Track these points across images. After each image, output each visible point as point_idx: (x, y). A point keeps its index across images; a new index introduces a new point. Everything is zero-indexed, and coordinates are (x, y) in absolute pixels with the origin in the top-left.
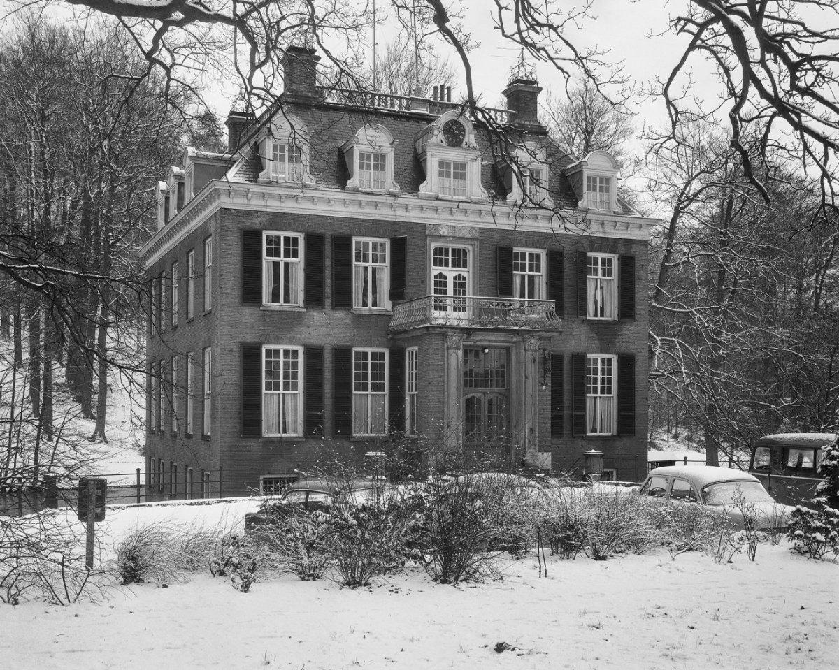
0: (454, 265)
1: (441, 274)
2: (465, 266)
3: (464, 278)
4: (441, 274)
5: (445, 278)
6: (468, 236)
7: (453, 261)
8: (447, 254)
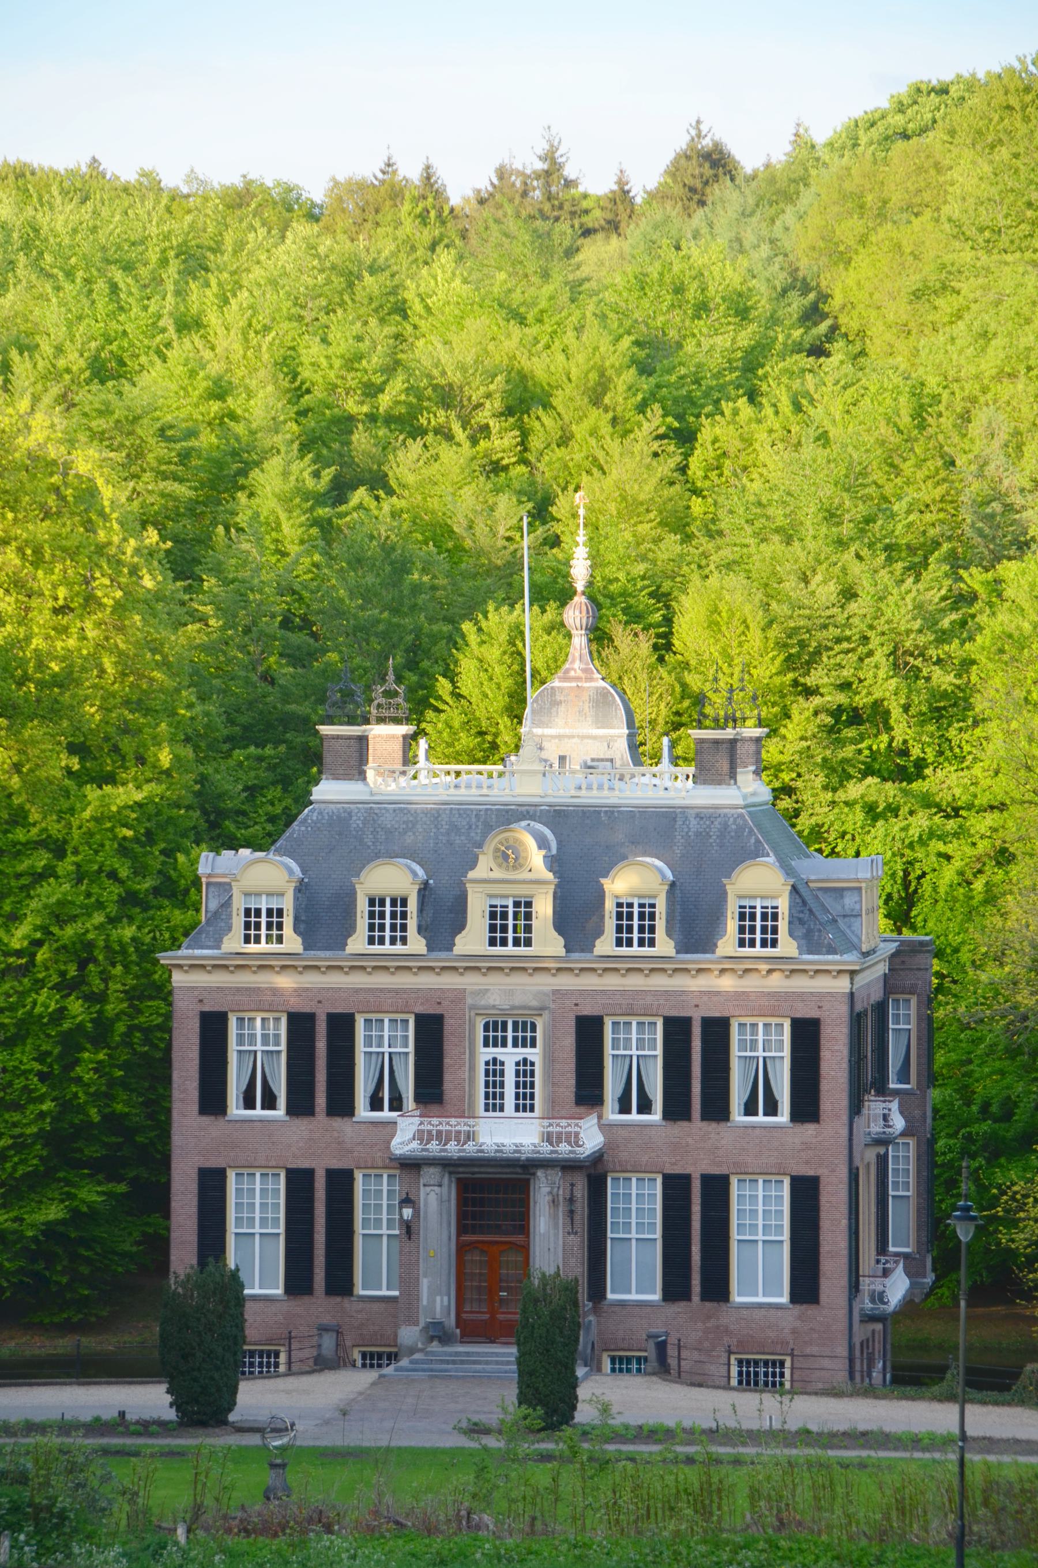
0: (515, 1045)
1: (495, 1060)
2: (533, 1045)
3: (532, 1064)
4: (495, 1060)
5: (502, 1064)
6: (534, 1003)
7: (515, 1039)
8: (504, 1029)
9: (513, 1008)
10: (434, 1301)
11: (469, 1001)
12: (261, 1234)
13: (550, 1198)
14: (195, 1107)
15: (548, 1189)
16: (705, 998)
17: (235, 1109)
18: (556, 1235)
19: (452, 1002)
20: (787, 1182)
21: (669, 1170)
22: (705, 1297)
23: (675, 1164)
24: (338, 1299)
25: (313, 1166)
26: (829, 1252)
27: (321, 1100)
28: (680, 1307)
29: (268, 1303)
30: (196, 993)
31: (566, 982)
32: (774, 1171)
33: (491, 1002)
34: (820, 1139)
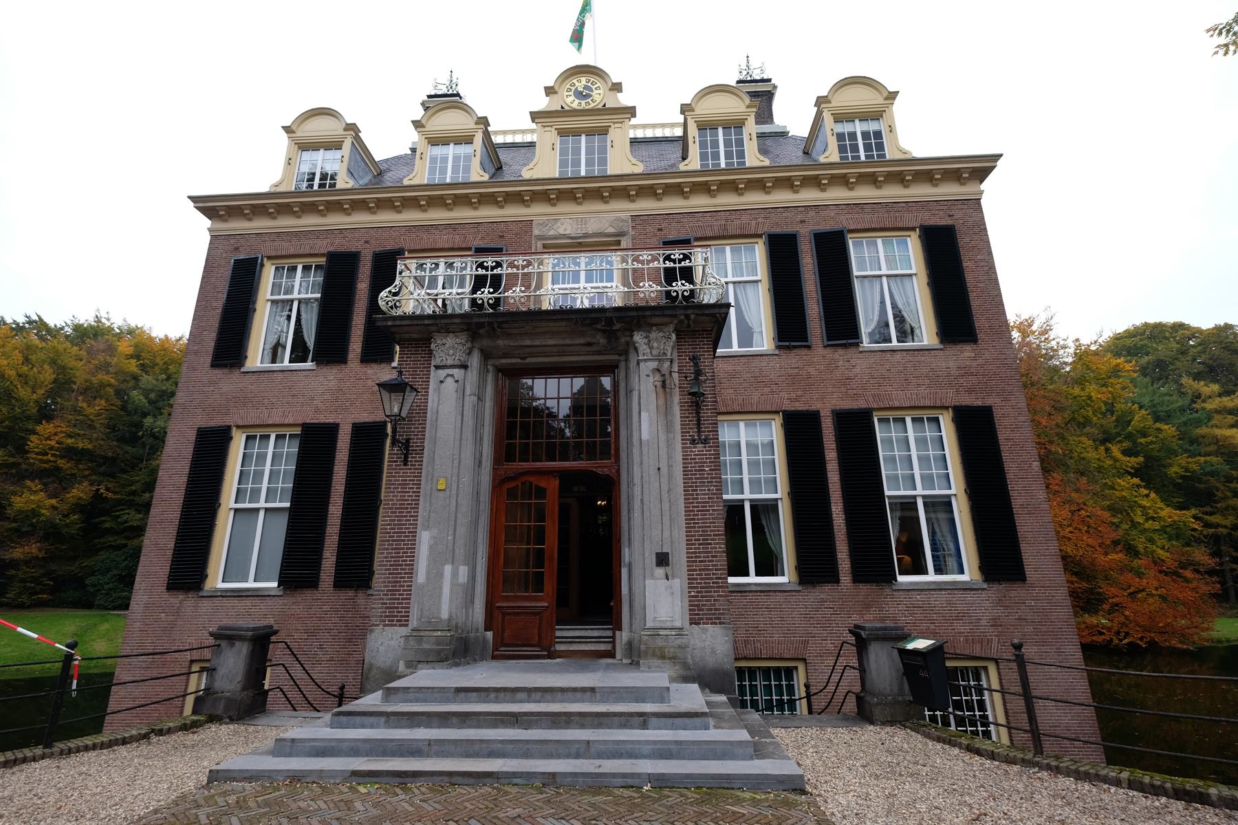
6: (611, 230)
9: (586, 236)
10: (440, 575)
11: (536, 232)
12: (267, 510)
13: (658, 377)
14: (208, 360)
15: (654, 365)
16: (812, 213)
17: (256, 357)
18: (669, 444)
19: (516, 235)
20: (946, 421)
21: (789, 406)
22: (859, 577)
23: (796, 400)
24: (351, 593)
25: (338, 421)
26: (1022, 506)
27: (356, 346)
28: (823, 592)
29: (257, 600)
30: (232, 241)
31: (646, 206)
32: (927, 403)
33: (561, 231)
34: (980, 361)
